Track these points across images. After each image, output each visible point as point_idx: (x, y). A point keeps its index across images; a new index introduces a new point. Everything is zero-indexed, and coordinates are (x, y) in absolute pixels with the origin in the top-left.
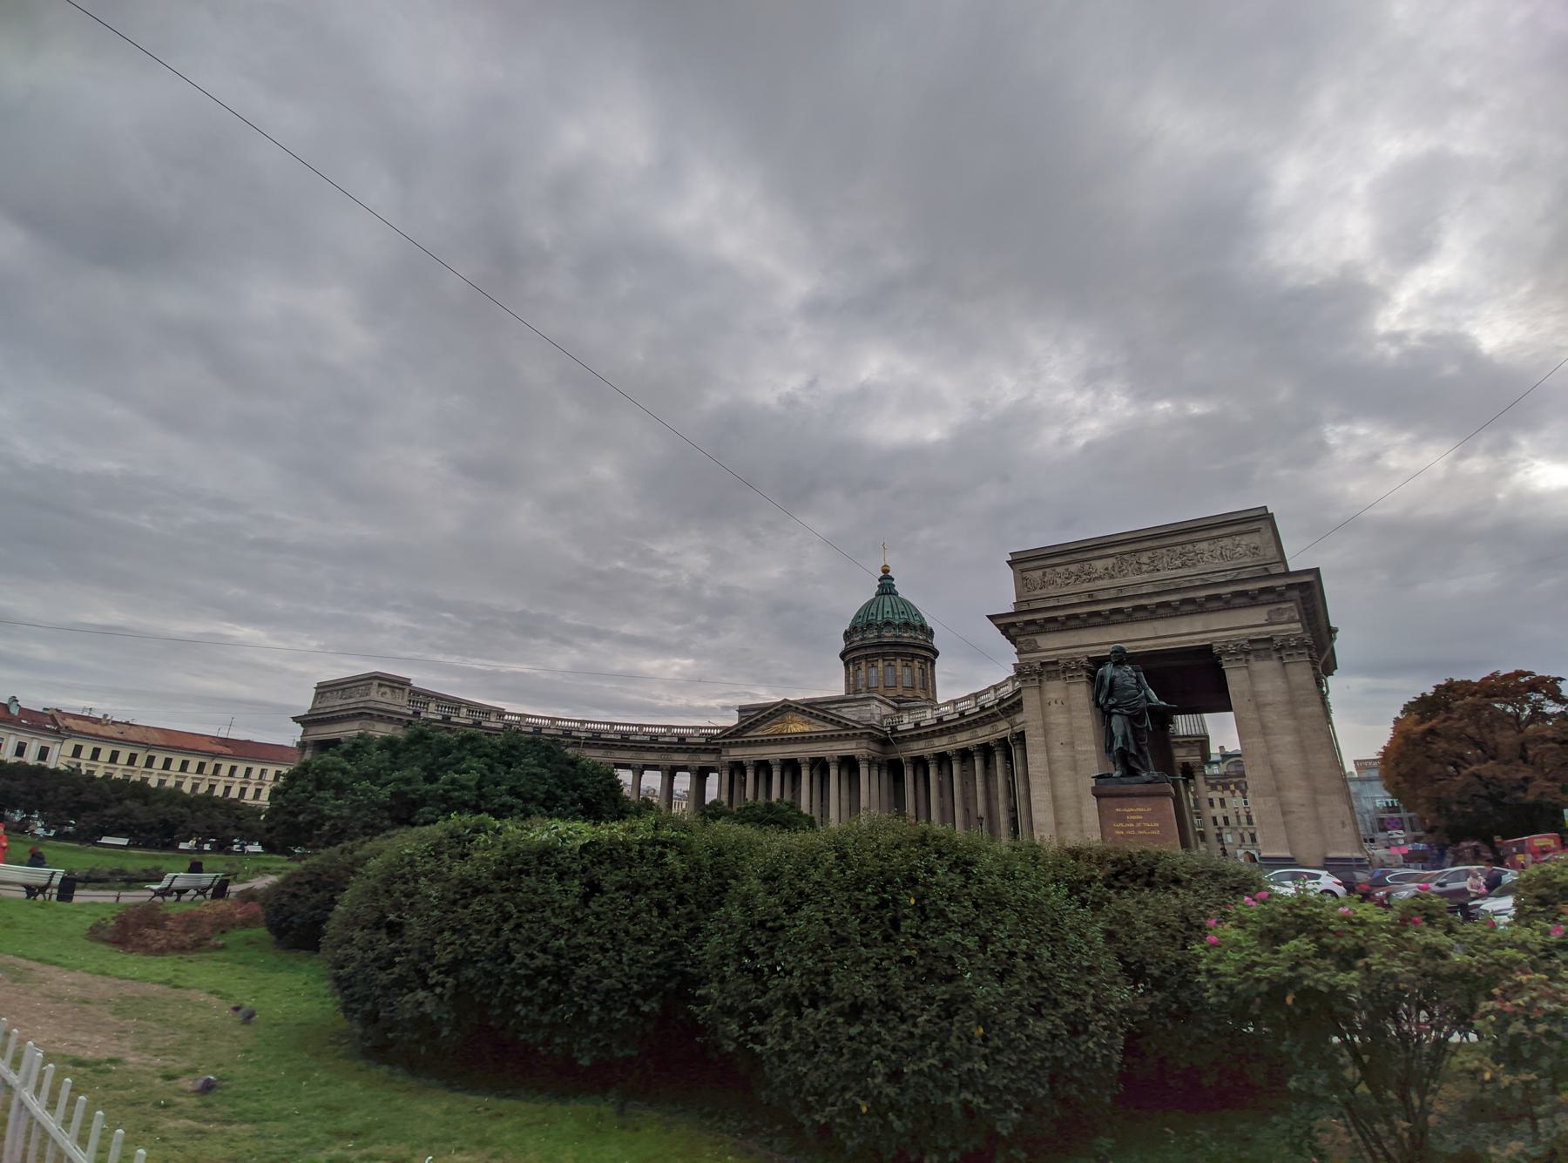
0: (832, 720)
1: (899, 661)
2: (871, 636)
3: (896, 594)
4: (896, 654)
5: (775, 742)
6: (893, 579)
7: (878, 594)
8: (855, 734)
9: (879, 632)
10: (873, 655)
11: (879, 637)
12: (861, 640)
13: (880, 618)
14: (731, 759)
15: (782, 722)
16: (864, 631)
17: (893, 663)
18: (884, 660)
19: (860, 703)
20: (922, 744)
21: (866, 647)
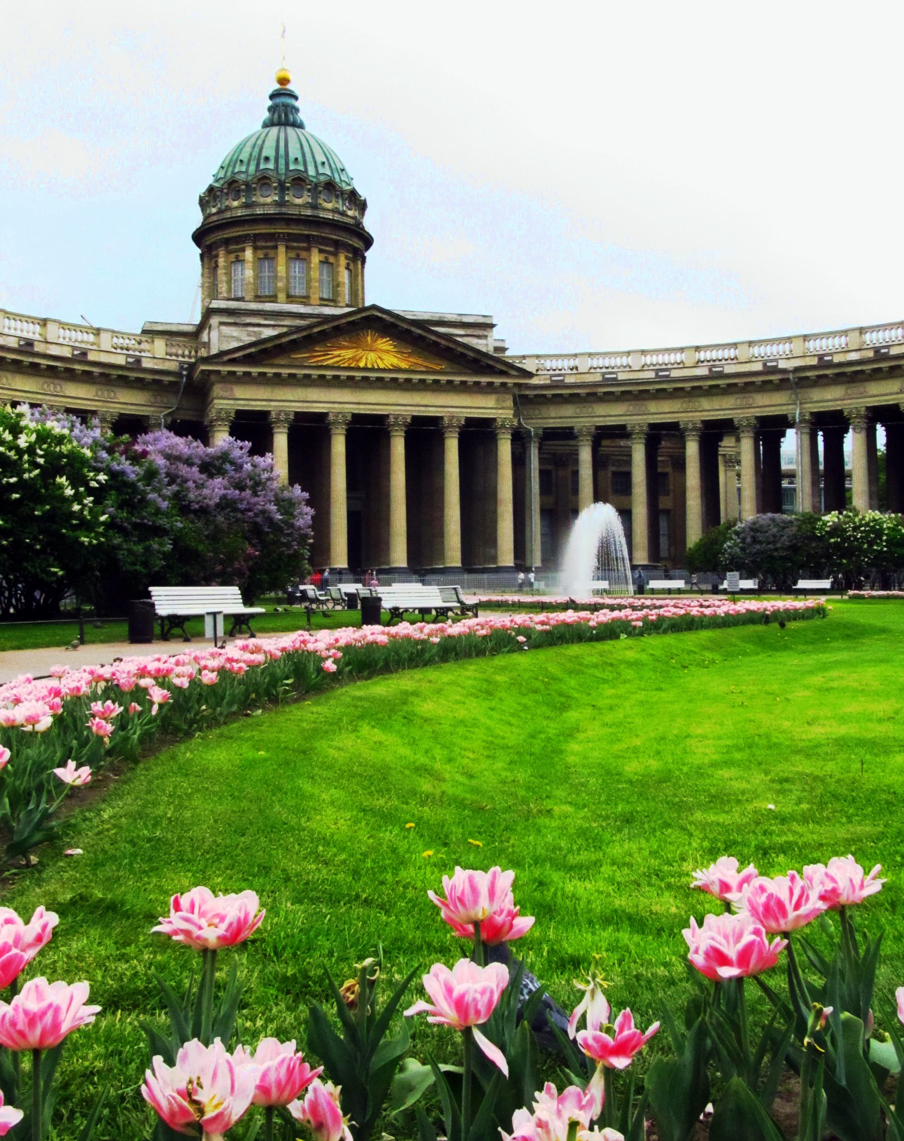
0: (463, 355)
2: (299, 201)
3: (301, 126)
4: (337, 244)
5: (351, 383)
6: (296, 98)
7: (266, 125)
8: (504, 384)
12: (277, 204)
13: (311, 172)
14: (243, 406)
15: (356, 343)
17: (332, 259)
18: (321, 251)
19: (469, 332)
20: (568, 411)
21: (290, 220)
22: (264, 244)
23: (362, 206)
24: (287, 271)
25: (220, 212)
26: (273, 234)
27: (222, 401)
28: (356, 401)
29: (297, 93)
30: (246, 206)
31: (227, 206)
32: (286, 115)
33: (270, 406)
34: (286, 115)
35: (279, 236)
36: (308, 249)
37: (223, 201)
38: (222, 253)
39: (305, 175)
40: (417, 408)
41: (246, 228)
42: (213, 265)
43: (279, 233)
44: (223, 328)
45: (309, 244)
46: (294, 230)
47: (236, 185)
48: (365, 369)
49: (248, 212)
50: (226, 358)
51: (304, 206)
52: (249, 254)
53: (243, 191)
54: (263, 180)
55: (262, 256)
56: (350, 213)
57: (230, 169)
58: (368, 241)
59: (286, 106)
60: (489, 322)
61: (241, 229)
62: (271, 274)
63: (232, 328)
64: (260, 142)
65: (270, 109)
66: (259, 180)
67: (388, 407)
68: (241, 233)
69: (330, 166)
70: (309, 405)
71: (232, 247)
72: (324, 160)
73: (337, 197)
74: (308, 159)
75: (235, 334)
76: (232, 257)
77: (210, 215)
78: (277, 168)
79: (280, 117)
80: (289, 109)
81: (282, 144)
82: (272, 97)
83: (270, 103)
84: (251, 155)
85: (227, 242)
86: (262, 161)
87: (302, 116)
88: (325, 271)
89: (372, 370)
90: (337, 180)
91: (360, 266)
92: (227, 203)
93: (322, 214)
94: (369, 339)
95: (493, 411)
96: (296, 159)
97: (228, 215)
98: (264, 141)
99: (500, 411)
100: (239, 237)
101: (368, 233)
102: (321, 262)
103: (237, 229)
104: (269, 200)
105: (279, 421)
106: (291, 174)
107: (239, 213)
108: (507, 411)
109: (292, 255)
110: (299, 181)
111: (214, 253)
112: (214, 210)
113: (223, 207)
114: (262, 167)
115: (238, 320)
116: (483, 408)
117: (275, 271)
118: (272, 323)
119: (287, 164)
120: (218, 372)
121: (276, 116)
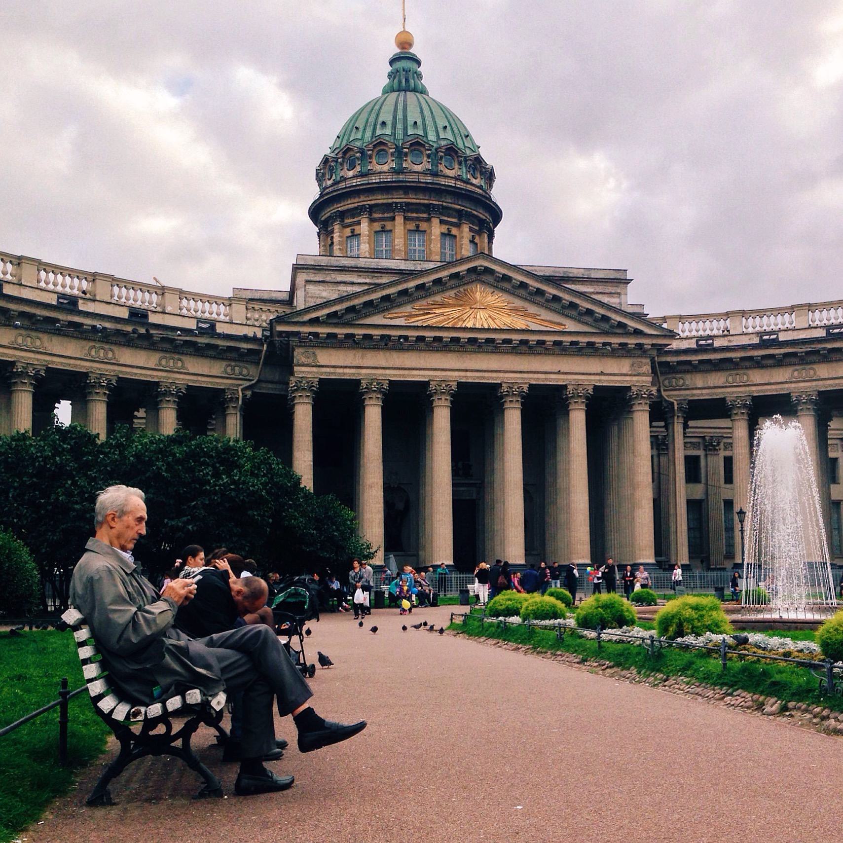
0: (589, 312)
1: (466, 228)
3: (423, 92)
4: (460, 214)
5: (454, 345)
6: (418, 63)
7: (385, 92)
8: (640, 346)
9: (435, 164)
10: (417, 208)
11: (435, 174)
12: (394, 171)
13: (432, 137)
14: (326, 373)
15: (462, 300)
16: (400, 154)
17: (454, 231)
18: (442, 222)
19: (599, 289)
21: (407, 189)
22: (380, 215)
23: (489, 176)
24: (406, 245)
25: (336, 183)
26: (391, 204)
27: (304, 369)
28: (463, 367)
29: (420, 56)
30: (362, 175)
31: (343, 176)
32: (407, 80)
33: (359, 374)
34: (407, 80)
35: (396, 207)
36: (428, 220)
37: (339, 170)
38: (337, 227)
39: (424, 139)
40: (536, 376)
41: (362, 198)
42: (330, 242)
43: (396, 203)
44: (311, 288)
45: (429, 214)
46: (412, 199)
47: (351, 153)
48: (472, 330)
49: (364, 180)
50: (307, 318)
51: (424, 173)
52: (364, 227)
53: (358, 158)
54: (379, 145)
55: (379, 229)
56: (474, 181)
57: (346, 138)
58: (496, 215)
59: (407, 71)
60: (622, 278)
61: (357, 200)
62: (389, 248)
63: (321, 288)
64: (377, 107)
65: (390, 76)
66: (375, 146)
67: (501, 375)
68: (356, 205)
69: (452, 129)
70: (406, 372)
71: (347, 221)
72: (447, 124)
73: (460, 163)
74: (427, 123)
75: (324, 294)
76: (348, 232)
77: (326, 188)
78: (394, 134)
79: (400, 82)
80: (411, 74)
81: (400, 107)
82: (392, 62)
83: (389, 69)
84: (367, 120)
85: (342, 215)
86: (378, 126)
87: (426, 82)
88: (448, 243)
89: (482, 330)
90: (461, 146)
91: (486, 240)
92: (342, 174)
93: (443, 181)
94: (478, 293)
95: (628, 378)
96: (415, 123)
97: (342, 185)
98: (380, 108)
99: (635, 378)
100: (356, 208)
101: (495, 203)
102: (443, 234)
103: (353, 201)
104: (385, 168)
105: (369, 390)
106: (410, 139)
107: (354, 182)
108: (644, 378)
109: (412, 226)
110: (418, 145)
111: (329, 229)
112: (329, 183)
113: (338, 179)
114: (378, 132)
115: (328, 279)
116: (614, 375)
117: (391, 242)
118: (368, 281)
119: (405, 129)
120: (297, 334)
121: (396, 81)
